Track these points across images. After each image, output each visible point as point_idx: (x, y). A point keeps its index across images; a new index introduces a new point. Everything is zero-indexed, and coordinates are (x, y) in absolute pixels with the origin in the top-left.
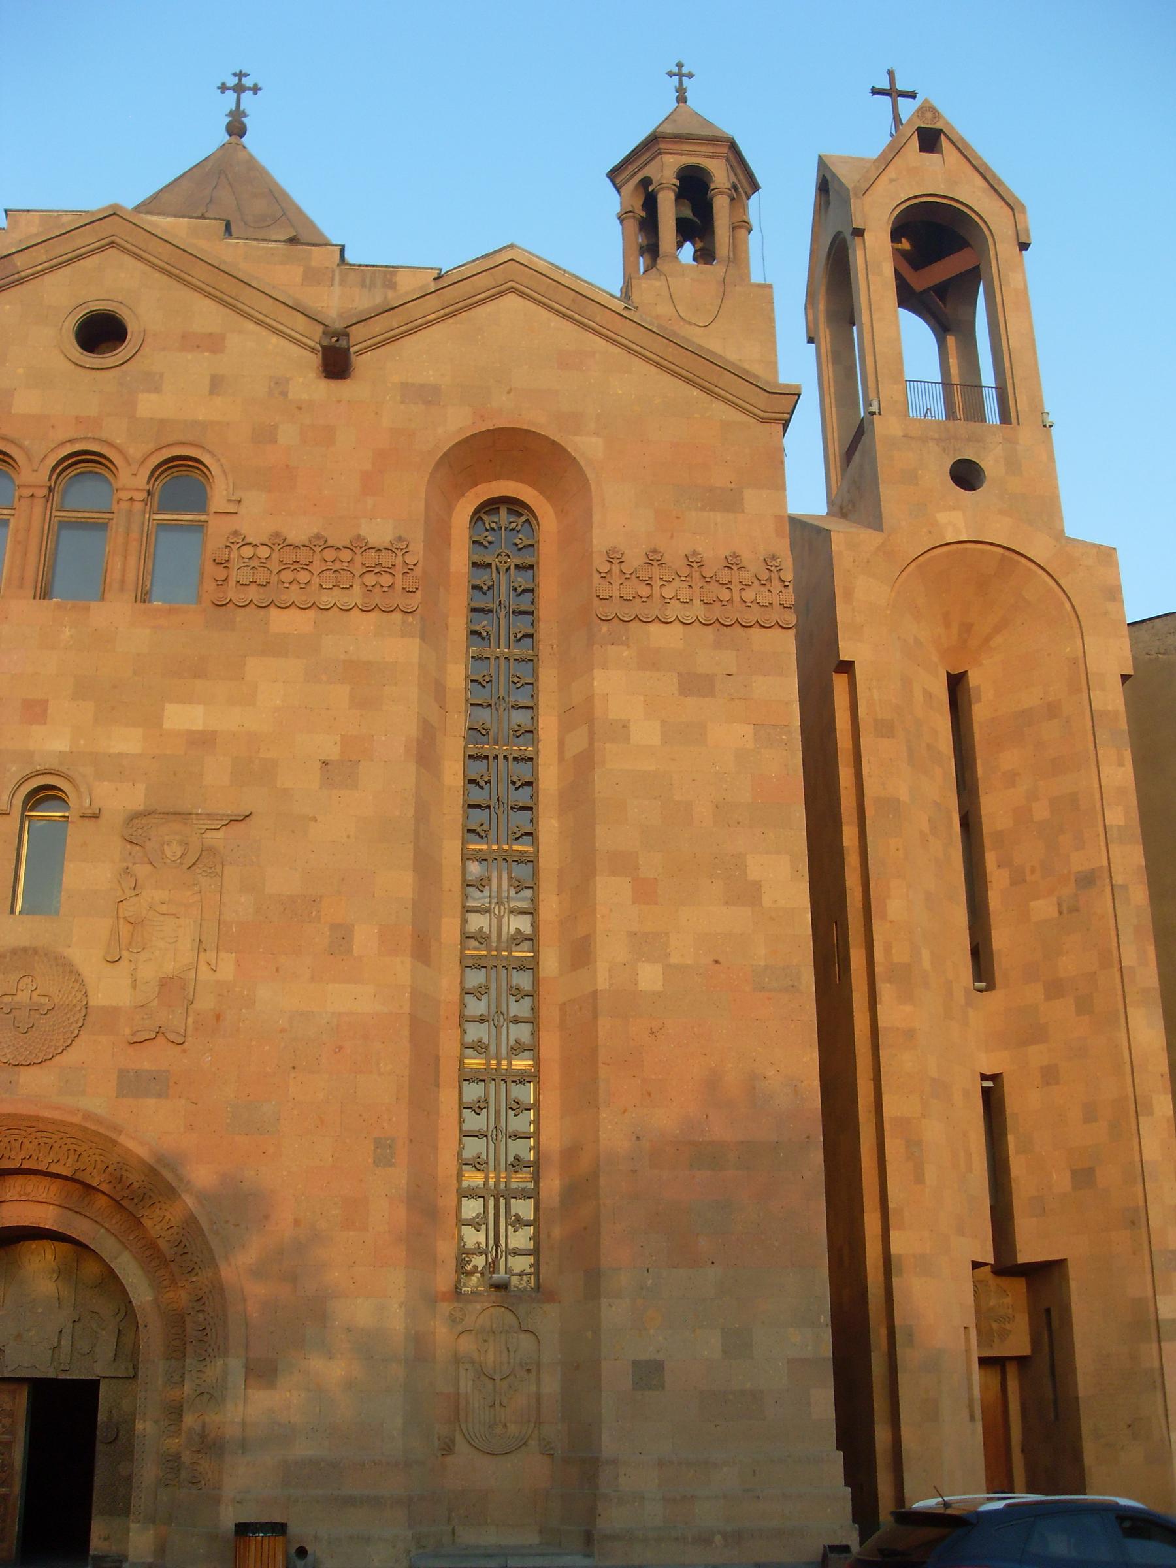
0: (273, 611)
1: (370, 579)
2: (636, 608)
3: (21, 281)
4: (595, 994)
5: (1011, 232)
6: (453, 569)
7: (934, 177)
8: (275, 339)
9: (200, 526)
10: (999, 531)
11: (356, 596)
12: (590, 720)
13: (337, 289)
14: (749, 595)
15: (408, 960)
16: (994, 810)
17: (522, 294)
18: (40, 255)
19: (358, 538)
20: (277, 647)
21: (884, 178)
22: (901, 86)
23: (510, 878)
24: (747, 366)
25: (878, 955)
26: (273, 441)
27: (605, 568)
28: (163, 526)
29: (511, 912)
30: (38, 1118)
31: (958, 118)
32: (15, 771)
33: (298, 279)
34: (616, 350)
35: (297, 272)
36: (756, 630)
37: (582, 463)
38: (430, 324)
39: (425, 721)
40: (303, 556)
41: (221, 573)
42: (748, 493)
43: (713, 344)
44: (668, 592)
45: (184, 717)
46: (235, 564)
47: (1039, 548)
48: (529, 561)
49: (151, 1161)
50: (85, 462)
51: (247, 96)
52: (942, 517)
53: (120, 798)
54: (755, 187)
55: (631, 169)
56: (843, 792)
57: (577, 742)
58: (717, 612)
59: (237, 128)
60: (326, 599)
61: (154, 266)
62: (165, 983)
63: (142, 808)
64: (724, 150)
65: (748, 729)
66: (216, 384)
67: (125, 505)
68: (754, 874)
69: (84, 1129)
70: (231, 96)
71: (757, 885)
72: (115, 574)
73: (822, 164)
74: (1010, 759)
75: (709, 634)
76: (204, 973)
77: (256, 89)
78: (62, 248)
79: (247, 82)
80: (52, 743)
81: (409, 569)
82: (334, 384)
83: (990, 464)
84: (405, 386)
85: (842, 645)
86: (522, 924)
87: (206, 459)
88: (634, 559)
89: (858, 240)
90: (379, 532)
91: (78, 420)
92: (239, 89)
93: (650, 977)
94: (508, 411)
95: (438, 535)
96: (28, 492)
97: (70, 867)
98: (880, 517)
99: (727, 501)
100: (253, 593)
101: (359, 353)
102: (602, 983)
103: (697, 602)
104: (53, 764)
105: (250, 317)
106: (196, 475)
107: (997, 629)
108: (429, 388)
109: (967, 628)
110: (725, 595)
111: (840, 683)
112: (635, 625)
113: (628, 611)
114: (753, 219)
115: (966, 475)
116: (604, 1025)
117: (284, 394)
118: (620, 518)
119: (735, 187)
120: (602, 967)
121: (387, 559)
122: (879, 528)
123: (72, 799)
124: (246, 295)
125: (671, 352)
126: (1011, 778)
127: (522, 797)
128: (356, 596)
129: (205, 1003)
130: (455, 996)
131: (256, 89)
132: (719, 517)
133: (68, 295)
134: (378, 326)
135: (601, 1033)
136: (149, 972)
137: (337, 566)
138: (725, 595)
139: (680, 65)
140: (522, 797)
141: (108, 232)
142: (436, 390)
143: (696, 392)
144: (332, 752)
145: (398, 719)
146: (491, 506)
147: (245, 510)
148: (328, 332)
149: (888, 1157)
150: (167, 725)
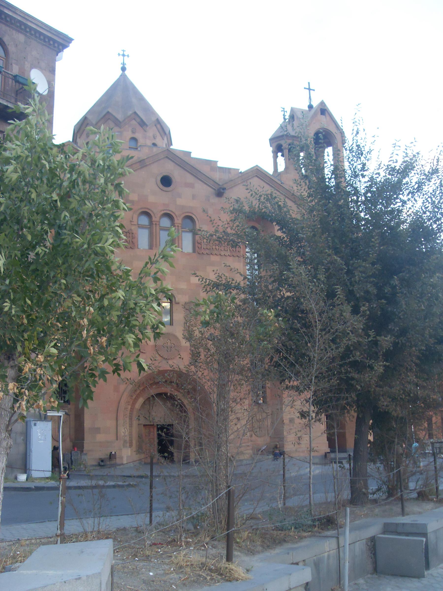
0: (211, 256)
3: (146, 166)
7: (322, 122)
8: (205, 186)
11: (228, 253)
17: (258, 177)
41: (200, 246)
46: (203, 244)
51: (126, 58)
59: (123, 69)
60: (222, 253)
61: (176, 164)
66: (194, 197)
70: (121, 57)
77: (128, 56)
79: (126, 53)
92: (124, 55)
150: (191, 282)
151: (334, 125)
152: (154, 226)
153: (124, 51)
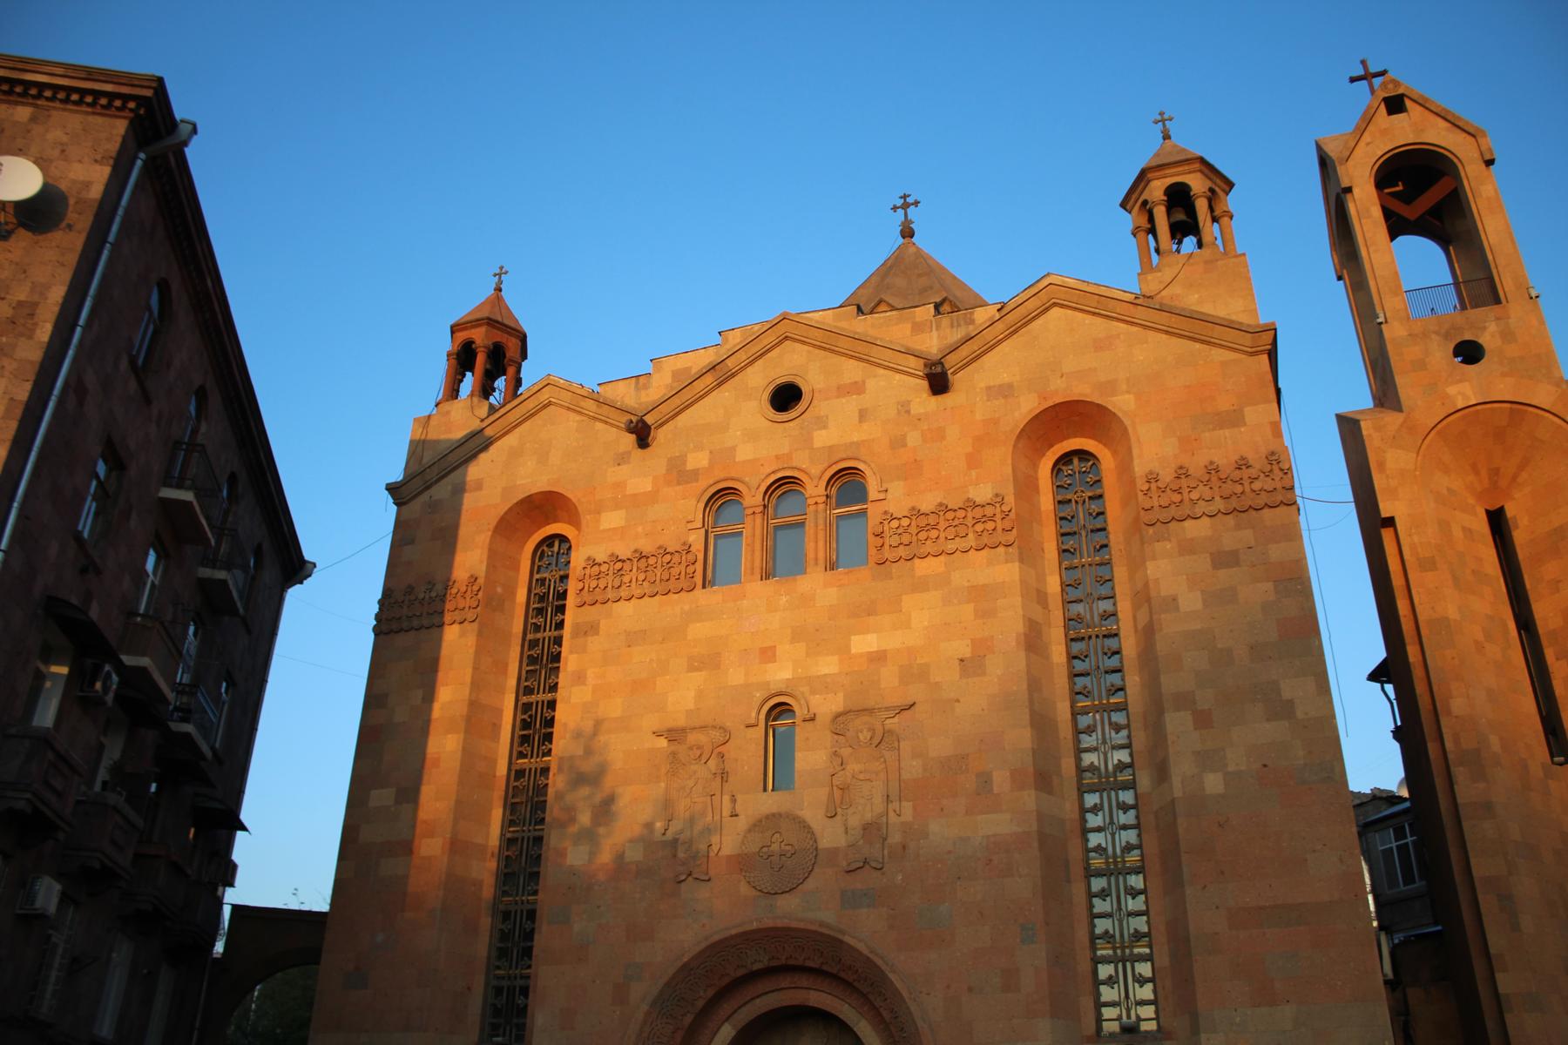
0: (916, 561)
1: (979, 527)
2: (1173, 511)
3: (733, 375)
4: (1173, 801)
5: (1477, 155)
6: (1043, 508)
7: (1403, 131)
8: (898, 376)
9: (863, 513)
10: (1504, 389)
11: (971, 540)
12: (1149, 600)
13: (935, 334)
14: (1257, 485)
15: (1033, 792)
16: (1545, 612)
17: (1062, 306)
18: (742, 356)
19: (968, 500)
20: (921, 586)
21: (1362, 144)
22: (1372, 70)
23: (1110, 723)
24: (1234, 318)
25: (1449, 745)
26: (905, 445)
27: (1146, 487)
28: (840, 517)
29: (1114, 748)
30: (789, 929)
31: (1409, 80)
32: (759, 695)
33: (908, 332)
34: (1135, 329)
35: (906, 328)
36: (1266, 511)
37: (1120, 415)
38: (1000, 342)
39: (1030, 620)
40: (932, 520)
41: (879, 541)
42: (1248, 411)
43: (1207, 309)
44: (1194, 496)
45: (864, 643)
46: (886, 534)
47: (1543, 395)
48: (1098, 492)
49: (866, 952)
50: (785, 485)
52: (1452, 390)
53: (827, 705)
54: (1231, 185)
55: (1134, 196)
56: (1403, 620)
57: (1143, 618)
58: (1234, 503)
59: (907, 233)
60: (951, 546)
61: (814, 346)
62: (867, 828)
63: (841, 710)
64: (1197, 166)
65: (1270, 586)
66: (863, 415)
67: (812, 508)
68: (1286, 695)
69: (822, 934)
70: (901, 212)
71: (1291, 702)
72: (811, 555)
73: (1319, 148)
74: (1551, 569)
75: (1230, 520)
76: (892, 817)
78: (755, 348)
80: (780, 674)
81: (1006, 515)
82: (940, 398)
83: (1488, 339)
84: (989, 388)
85: (1381, 506)
86: (1123, 756)
87: (861, 466)
88: (1167, 476)
89: (1348, 196)
90: (982, 493)
91: (777, 457)
93: (1213, 783)
94: (1063, 389)
95: (1026, 487)
96: (750, 511)
97: (798, 755)
98: (1399, 401)
99: (1233, 419)
100: (902, 551)
101: (954, 373)
102: (1178, 793)
103: (1217, 498)
104: (782, 687)
105: (879, 365)
106: (858, 478)
107: (1522, 467)
108: (1005, 384)
109: (1495, 472)
110: (1239, 489)
111: (1387, 535)
112: (1173, 525)
113: (1165, 516)
114: (1231, 208)
115: (1469, 352)
116: (1182, 824)
117: (908, 412)
118: (1152, 448)
119: (1211, 190)
120: (1176, 782)
121: (989, 511)
122: (1401, 410)
123: (796, 708)
124: (874, 351)
125: (1175, 321)
126: (1555, 585)
127: (1113, 662)
128: (971, 540)
129: (895, 838)
130: (1076, 815)
131: (916, 203)
132: (1227, 432)
133: (762, 378)
134: (965, 351)
135: (1181, 830)
136: (855, 821)
137: (956, 522)
138: (1239, 489)
139: (1162, 114)
140: (1113, 662)
141: (785, 331)
142: (1010, 386)
143: (1197, 345)
144: (965, 650)
145: (1009, 622)
146: (1066, 458)
147: (891, 496)
148: (930, 364)
149: (1483, 910)
151: (1442, 124)
152: (748, 520)
153: (905, 197)
